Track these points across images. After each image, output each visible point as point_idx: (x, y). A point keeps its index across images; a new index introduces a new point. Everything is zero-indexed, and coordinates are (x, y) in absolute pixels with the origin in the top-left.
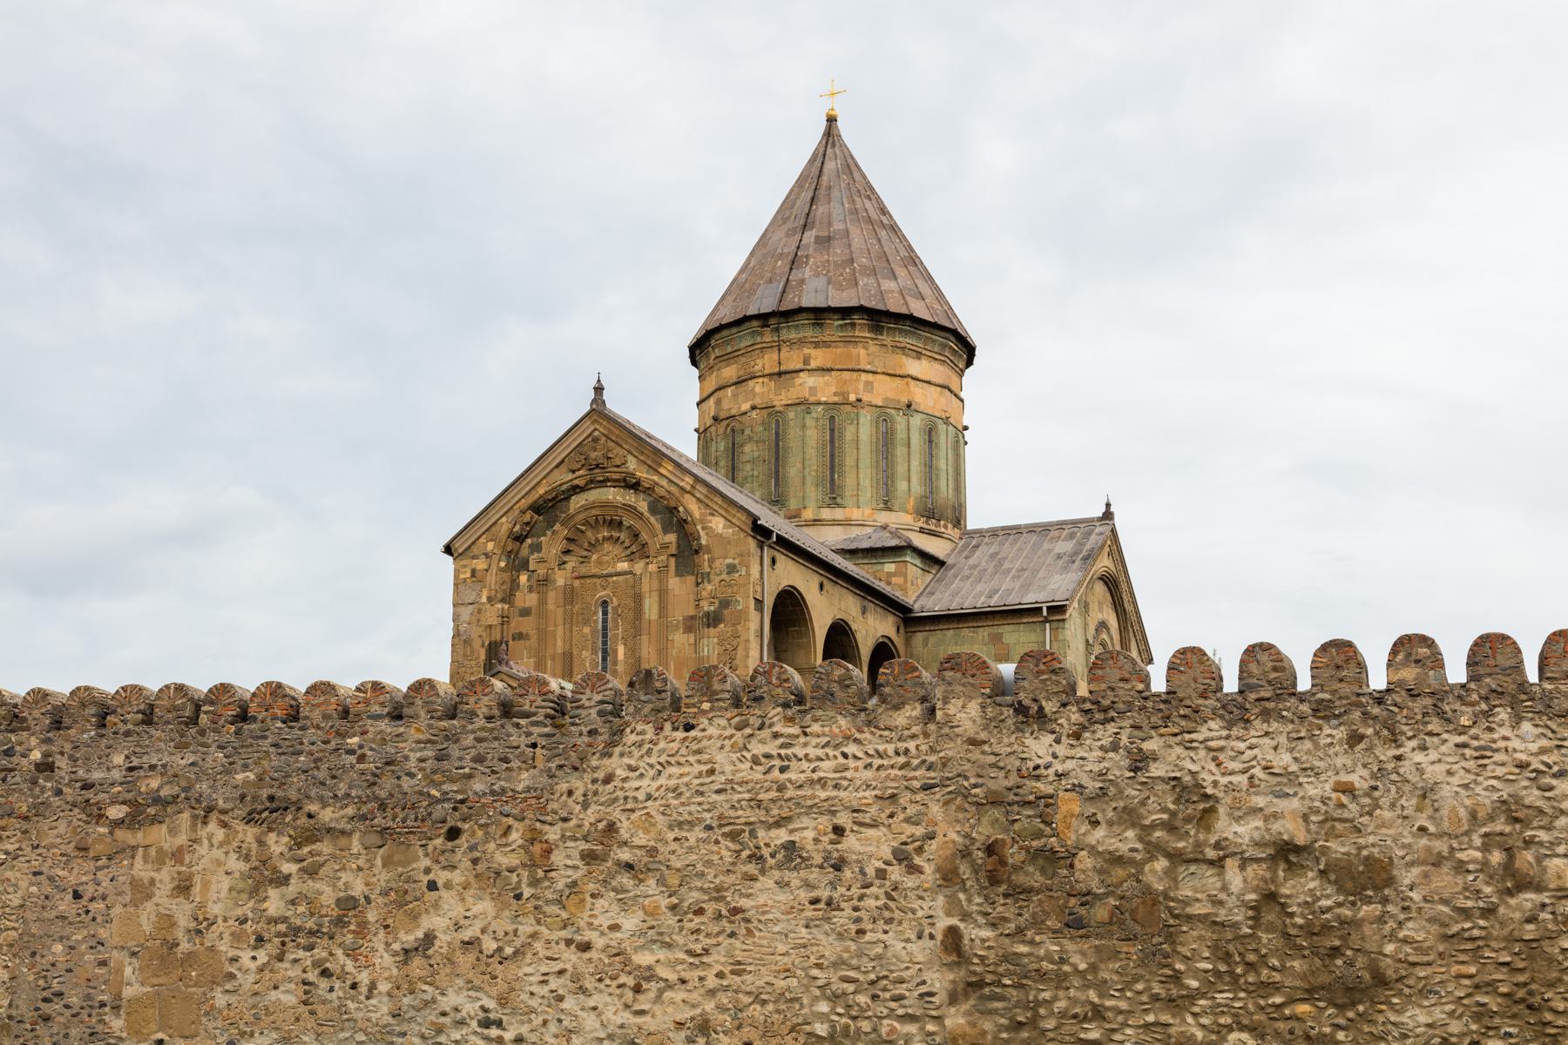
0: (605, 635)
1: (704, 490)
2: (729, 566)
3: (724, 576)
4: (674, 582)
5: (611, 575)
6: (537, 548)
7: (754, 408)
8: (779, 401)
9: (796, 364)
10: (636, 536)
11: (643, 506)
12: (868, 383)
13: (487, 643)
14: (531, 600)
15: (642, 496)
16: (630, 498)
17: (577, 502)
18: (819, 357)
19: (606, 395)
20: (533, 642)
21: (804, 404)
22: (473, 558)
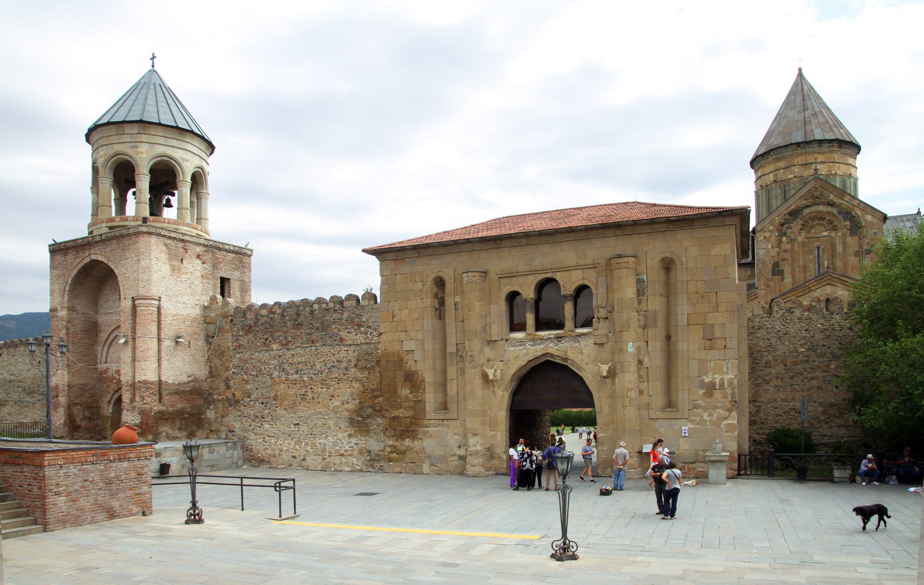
2: (874, 232)
4: (849, 239)
6: (789, 228)
7: (795, 177)
10: (832, 223)
11: (835, 212)
12: (838, 167)
14: (788, 247)
15: (834, 208)
16: (830, 209)
17: (806, 211)
18: (820, 158)
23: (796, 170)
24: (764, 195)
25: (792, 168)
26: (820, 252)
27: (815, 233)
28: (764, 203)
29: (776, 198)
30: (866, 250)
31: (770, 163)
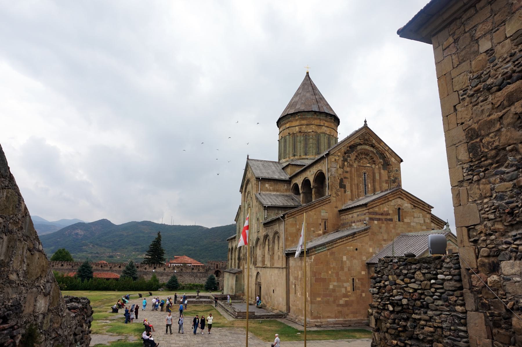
0: (365, 181)
1: (391, 151)
2: (396, 170)
3: (395, 172)
4: (382, 171)
5: (366, 167)
7: (313, 131)
8: (319, 131)
9: (322, 124)
10: (373, 158)
11: (375, 152)
13: (340, 178)
14: (348, 169)
15: (374, 149)
16: (372, 149)
17: (359, 147)
18: (326, 124)
19: (367, 123)
20: (349, 180)
21: (325, 133)
22: (335, 156)
23: (313, 127)
24: (291, 139)
25: (311, 126)
26: (366, 177)
27: (363, 163)
28: (291, 144)
29: (300, 142)
30: (393, 180)
31: (297, 120)
